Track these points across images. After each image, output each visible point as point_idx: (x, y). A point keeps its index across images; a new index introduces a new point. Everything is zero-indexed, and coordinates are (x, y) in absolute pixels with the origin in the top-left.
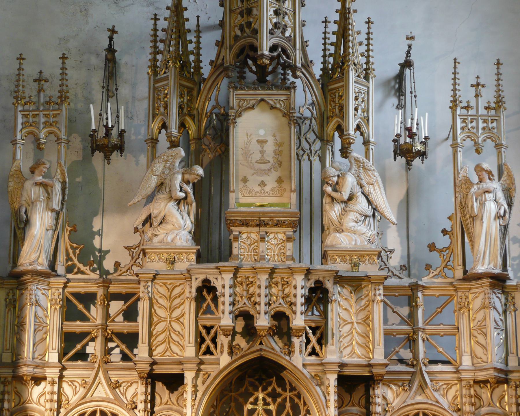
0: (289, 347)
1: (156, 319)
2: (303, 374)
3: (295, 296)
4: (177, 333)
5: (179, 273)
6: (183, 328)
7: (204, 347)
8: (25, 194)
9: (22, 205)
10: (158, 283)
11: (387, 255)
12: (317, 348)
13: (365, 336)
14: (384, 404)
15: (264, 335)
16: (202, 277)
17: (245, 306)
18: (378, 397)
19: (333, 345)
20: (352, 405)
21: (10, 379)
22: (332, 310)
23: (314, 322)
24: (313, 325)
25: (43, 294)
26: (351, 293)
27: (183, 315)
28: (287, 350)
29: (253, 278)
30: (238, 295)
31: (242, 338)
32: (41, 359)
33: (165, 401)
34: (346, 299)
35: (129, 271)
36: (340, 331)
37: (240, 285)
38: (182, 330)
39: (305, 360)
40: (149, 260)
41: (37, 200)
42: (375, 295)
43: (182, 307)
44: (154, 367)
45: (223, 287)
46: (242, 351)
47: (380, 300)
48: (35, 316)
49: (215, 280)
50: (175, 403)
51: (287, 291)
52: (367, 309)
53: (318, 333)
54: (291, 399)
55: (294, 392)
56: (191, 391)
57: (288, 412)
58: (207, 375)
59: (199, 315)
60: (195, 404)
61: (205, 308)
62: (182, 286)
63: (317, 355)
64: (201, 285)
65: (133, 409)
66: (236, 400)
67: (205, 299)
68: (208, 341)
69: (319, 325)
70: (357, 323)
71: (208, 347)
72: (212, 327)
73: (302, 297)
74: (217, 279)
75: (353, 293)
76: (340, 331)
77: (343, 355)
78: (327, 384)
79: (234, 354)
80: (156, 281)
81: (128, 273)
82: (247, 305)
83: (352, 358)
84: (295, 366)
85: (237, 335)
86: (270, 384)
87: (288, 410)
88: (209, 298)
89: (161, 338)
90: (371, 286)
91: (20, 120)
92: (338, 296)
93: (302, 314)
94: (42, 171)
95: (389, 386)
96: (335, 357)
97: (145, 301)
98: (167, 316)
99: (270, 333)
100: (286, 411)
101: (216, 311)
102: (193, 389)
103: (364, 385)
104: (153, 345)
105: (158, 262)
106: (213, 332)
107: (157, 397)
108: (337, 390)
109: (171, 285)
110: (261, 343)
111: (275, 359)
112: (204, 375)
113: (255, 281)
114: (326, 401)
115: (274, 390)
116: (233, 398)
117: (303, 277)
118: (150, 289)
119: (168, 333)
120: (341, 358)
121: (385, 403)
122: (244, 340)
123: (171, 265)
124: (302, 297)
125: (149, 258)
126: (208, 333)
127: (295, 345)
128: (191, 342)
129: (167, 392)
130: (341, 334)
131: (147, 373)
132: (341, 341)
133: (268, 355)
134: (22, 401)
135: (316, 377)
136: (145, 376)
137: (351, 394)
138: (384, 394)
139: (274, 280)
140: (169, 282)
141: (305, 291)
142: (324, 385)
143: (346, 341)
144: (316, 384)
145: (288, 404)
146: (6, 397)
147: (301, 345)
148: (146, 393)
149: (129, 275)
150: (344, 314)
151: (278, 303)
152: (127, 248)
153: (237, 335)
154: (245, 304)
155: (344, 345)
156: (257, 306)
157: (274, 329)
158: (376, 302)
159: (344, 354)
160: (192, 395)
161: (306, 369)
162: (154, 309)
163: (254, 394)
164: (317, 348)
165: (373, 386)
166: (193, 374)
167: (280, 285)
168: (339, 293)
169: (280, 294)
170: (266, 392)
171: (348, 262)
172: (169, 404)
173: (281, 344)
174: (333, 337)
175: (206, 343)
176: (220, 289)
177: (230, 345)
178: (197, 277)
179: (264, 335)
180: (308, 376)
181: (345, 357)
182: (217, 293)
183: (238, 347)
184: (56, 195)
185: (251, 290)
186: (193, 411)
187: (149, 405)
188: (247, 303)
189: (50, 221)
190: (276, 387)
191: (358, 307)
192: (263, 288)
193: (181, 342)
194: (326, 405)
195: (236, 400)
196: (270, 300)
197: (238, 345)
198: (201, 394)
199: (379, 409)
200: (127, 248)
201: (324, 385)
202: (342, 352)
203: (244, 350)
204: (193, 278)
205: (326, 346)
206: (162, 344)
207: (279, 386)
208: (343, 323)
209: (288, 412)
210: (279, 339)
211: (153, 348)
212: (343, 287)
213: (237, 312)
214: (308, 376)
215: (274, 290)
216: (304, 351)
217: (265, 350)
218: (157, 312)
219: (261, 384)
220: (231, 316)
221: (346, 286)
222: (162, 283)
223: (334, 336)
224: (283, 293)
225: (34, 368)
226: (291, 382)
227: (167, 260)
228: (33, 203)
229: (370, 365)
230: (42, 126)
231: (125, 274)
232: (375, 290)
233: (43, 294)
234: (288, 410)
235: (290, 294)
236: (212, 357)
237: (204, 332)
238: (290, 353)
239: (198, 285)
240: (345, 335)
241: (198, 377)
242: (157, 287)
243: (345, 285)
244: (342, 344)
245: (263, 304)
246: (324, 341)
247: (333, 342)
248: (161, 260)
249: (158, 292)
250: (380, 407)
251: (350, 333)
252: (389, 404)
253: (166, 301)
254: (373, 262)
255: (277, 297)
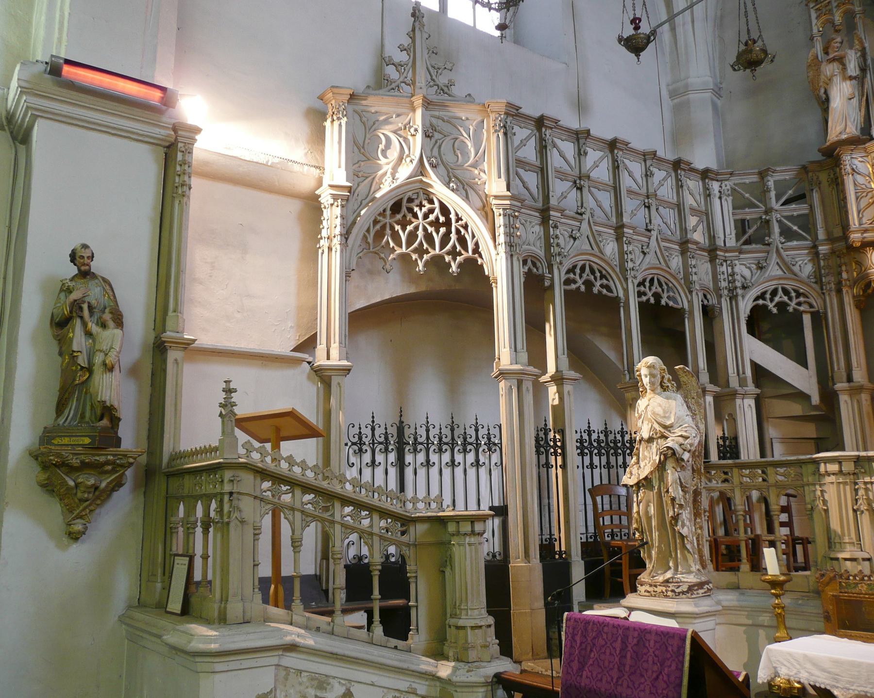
8: (822, 77)
9: (821, 86)
21: (845, 251)
25: (862, 162)
32: (871, 224)
41: (833, 75)
48: (855, 184)
91: (814, 15)
94: (834, 47)
134: (863, 269)
146: (844, 268)
184: (850, 62)
189: (850, 90)
225: (862, 234)
228: (830, 80)
230: (835, 10)
233: (862, 162)
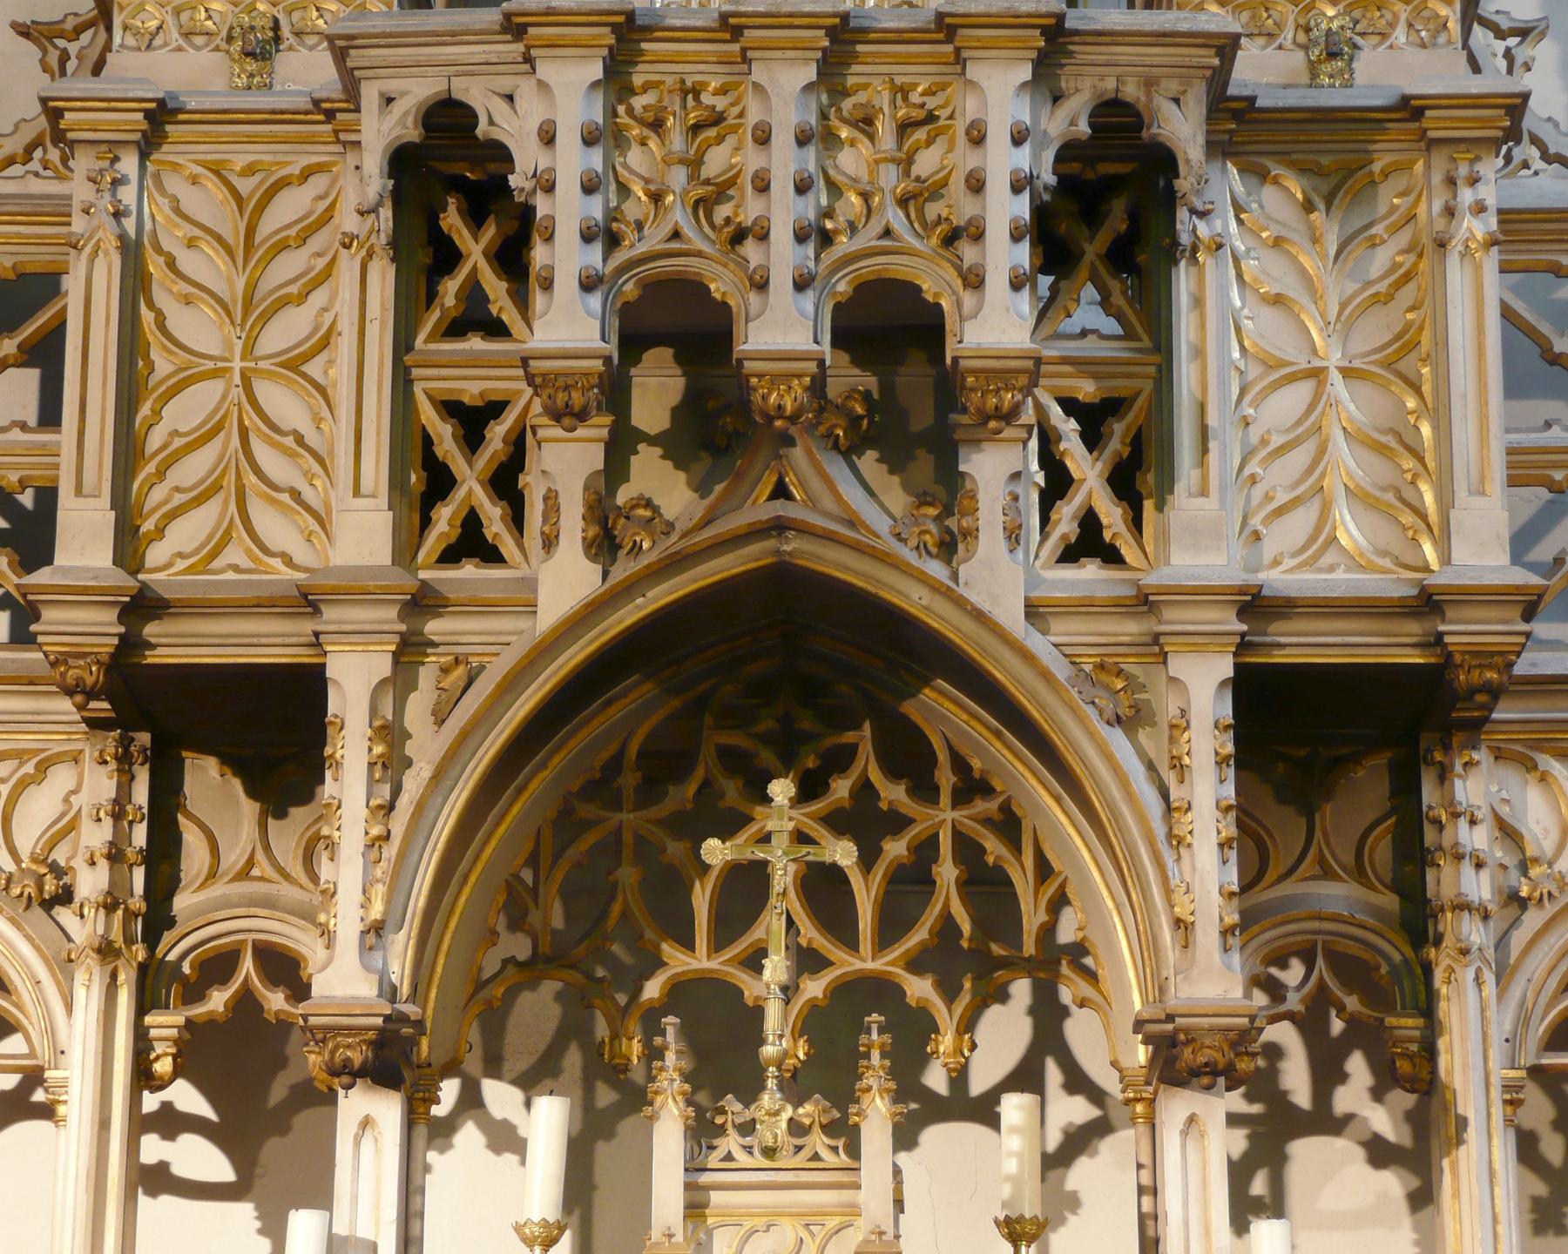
0: (948, 511)
1: (163, 364)
2: (1028, 657)
3: (976, 185)
4: (289, 441)
5: (303, 103)
6: (325, 412)
7: (445, 518)
10: (176, 167)
11: (1508, 54)
12: (1112, 516)
13: (1394, 444)
14: (1504, 867)
15: (789, 406)
16: (420, 90)
17: (675, 245)
18: (1473, 822)
19: (1204, 493)
20: (1317, 870)
22: (1198, 302)
23: (1096, 377)
24: (1086, 390)
26: (1308, 207)
27: (325, 343)
28: (932, 527)
29: (722, 91)
30: (638, 189)
31: (669, 464)
33: (232, 858)
34: (1278, 242)
35: (38, 153)
36: (1246, 422)
37: (646, 132)
38: (317, 421)
39: (1044, 581)
40: (130, 41)
42: (1450, 212)
43: (319, 298)
44: (151, 630)
45: (548, 137)
46: (666, 534)
47: (1479, 236)
49: (500, 108)
50: (298, 871)
51: (927, 163)
52: (1408, 294)
53: (1118, 433)
54: (967, 849)
55: (982, 806)
56: (365, 759)
57: (947, 924)
58: (460, 671)
59: (419, 343)
60: (387, 837)
61: (450, 301)
62: (318, 183)
63: (1111, 556)
64: (413, 134)
65: (48, 905)
66: (645, 851)
67: (446, 257)
68: (471, 487)
69: (1121, 387)
70: (1347, 373)
71: (472, 522)
72: (495, 409)
73: (1016, 189)
74: (510, 98)
75: (1321, 206)
76: (1246, 422)
77: (1267, 558)
78: (1173, 710)
79: (622, 553)
80: (165, 153)
81: (34, 165)
82: (689, 241)
83: (1320, 570)
84: (979, 616)
85: (642, 447)
86: (841, 760)
87: (946, 905)
88: (475, 249)
89: (194, 468)
90: (1428, 166)
92: (1233, 226)
93: (1016, 285)
95: (1531, 766)
96: (1218, 559)
97: (100, 263)
98: (229, 346)
99: (829, 434)
100: (935, 909)
101: (517, 316)
102: (379, 749)
103: (1381, 760)
104: (147, 507)
105: (179, 49)
106: (497, 433)
107: (192, 838)
108: (1230, 748)
109: (258, 177)
110: (781, 492)
111: (864, 576)
112: (445, 670)
113: (736, 110)
114: (1169, 809)
115: (865, 789)
116: (627, 838)
117: (1025, 72)
118: (128, 195)
119: (235, 441)
120: (1257, 571)
121: (1511, 861)
122: (682, 476)
123: (252, 66)
124: (1016, 189)
125: (126, 28)
126: (472, 439)
127: (981, 496)
128: (367, 483)
129: (249, 809)
130: (1255, 434)
131: (105, 659)
132: (1253, 480)
133: (820, 559)
135: (1103, 677)
136: (90, 680)
137: (1309, 811)
138: (1504, 811)
139: (847, 104)
140: (240, 161)
141: (1036, 157)
142: (1154, 724)
143: (1280, 477)
144: (1109, 714)
145: (947, 872)
147: (1016, 498)
148: (119, 810)
149: (37, 174)
150: (1263, 326)
151: (876, 227)
152: (24, 31)
153: (642, 447)
154: (676, 235)
155: (1268, 498)
156: (751, 249)
157: (859, 410)
158: (1456, 246)
159: (1269, 548)
160: (371, 782)
161: (1045, 632)
162: (151, 305)
163: (749, 819)
164: (1112, 516)
165: (1438, 756)
166: (382, 665)
167: (885, 129)
168: (1238, 209)
169: (889, 177)
170: (818, 806)
171: (1288, 35)
172: (261, 879)
173: (897, 498)
174: (1205, 451)
175: (459, 494)
176: (527, 158)
177: (599, 500)
178: (392, 86)
179: (789, 406)
180: (1060, 670)
181: (1276, 563)
182: (513, 181)
183: (648, 513)
185: (717, 161)
186: (378, 873)
187: (139, 876)
188: (688, 230)
190: (875, 776)
191: (1352, 287)
192: (783, 139)
193: (309, 495)
194: (1170, 835)
195: (645, 851)
196: (828, 213)
197: (648, 504)
198: (427, 773)
199: (1479, 887)
200: (24, 31)
201: (1154, 724)
202: (1257, 536)
203: (680, 527)
204: (370, 94)
205: (1160, 507)
206: (199, 500)
207: (893, 771)
208: (1261, 377)
209: (947, 924)
210: (885, 467)
211: (148, 526)
212: (1263, 176)
213: (629, 287)
214: (1060, 670)
215: (851, 161)
216: (1036, 536)
217: (805, 530)
218: (170, 324)
219: (787, 763)
220: (595, 301)
221: (1276, 170)
222: (198, 163)
223: (1212, 445)
224: (907, 173)
226: (964, 751)
227: (230, 39)
229: (1428, 603)
231: (16, 170)
232: (1451, 182)
234: (946, 905)
235: (944, 183)
236: (495, 573)
237: (444, 434)
238: (948, 548)
239: (397, 132)
240: (1277, 441)
241: (413, 686)
242: (174, 184)
243: (1268, 162)
244: (1258, 493)
245: (782, 234)
246: (1147, 480)
247: (1205, 478)
248: (199, 40)
249: (178, 211)
250: (1485, 875)
251: (1309, 429)
252: (1536, 861)
253: (221, 261)
254: (1434, 37)
255: (866, 196)
